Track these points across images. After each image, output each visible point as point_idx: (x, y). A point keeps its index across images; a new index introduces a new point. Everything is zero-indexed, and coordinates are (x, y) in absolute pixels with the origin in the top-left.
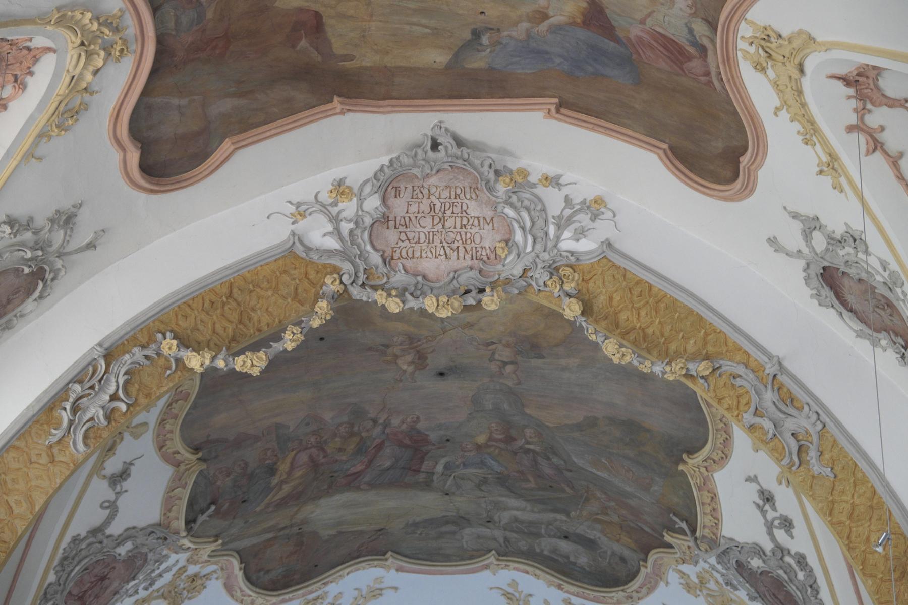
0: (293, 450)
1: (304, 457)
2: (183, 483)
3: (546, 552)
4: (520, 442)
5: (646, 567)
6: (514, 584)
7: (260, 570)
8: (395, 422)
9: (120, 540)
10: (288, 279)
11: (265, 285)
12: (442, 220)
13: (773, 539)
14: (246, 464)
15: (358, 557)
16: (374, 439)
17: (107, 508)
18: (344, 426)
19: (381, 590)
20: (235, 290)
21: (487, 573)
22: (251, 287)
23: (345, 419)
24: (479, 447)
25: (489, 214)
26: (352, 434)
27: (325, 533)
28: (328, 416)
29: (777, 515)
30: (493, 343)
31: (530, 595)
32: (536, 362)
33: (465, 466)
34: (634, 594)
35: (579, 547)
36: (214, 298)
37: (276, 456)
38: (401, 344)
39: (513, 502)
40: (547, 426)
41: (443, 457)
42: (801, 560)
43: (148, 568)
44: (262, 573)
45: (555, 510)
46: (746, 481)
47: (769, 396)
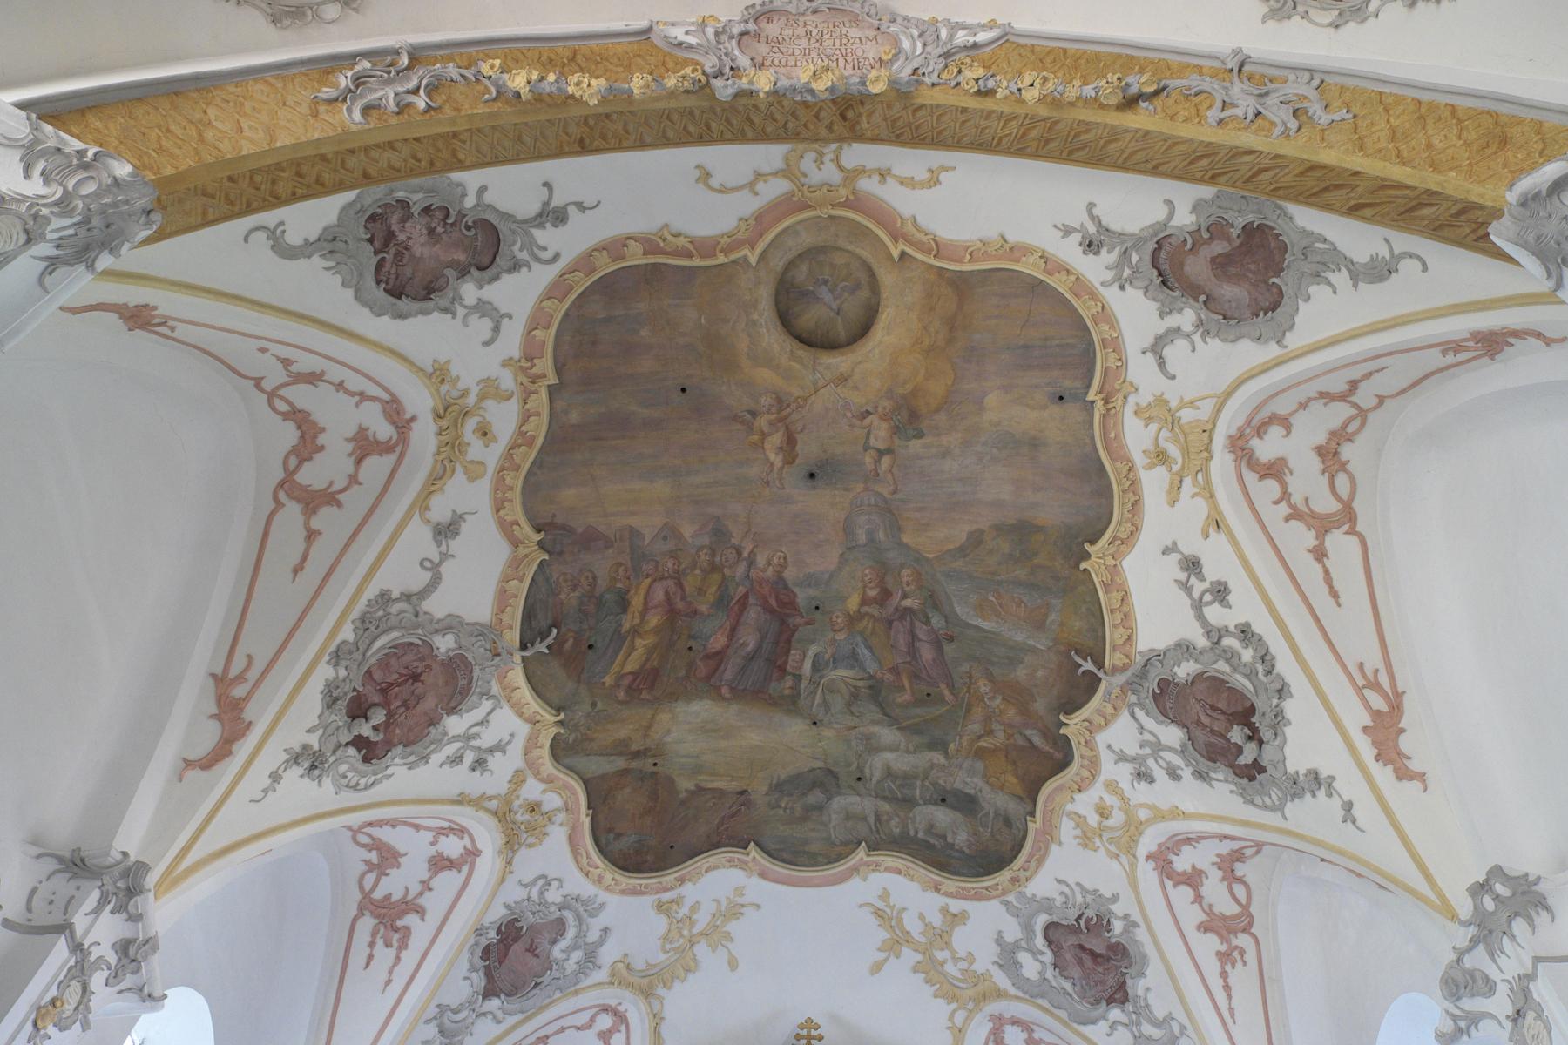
0: (648, 576)
1: (659, 595)
2: (521, 573)
3: (921, 835)
4: (895, 599)
5: (1035, 822)
6: (885, 895)
7: (610, 830)
8: (761, 560)
10: (643, 63)
11: (615, 60)
12: (820, 41)
14: (595, 578)
15: (717, 848)
16: (738, 584)
17: (427, 569)
18: (705, 551)
19: (743, 906)
20: (579, 57)
22: (598, 59)
23: (706, 540)
24: (853, 619)
25: (871, 33)
26: (714, 568)
28: (687, 531)
29: (1207, 585)
30: (868, 413)
31: (904, 909)
32: (915, 445)
34: (1022, 874)
36: (553, 56)
37: (629, 579)
39: (887, 735)
40: (927, 560)
41: (812, 642)
42: (1245, 633)
46: (1163, 553)
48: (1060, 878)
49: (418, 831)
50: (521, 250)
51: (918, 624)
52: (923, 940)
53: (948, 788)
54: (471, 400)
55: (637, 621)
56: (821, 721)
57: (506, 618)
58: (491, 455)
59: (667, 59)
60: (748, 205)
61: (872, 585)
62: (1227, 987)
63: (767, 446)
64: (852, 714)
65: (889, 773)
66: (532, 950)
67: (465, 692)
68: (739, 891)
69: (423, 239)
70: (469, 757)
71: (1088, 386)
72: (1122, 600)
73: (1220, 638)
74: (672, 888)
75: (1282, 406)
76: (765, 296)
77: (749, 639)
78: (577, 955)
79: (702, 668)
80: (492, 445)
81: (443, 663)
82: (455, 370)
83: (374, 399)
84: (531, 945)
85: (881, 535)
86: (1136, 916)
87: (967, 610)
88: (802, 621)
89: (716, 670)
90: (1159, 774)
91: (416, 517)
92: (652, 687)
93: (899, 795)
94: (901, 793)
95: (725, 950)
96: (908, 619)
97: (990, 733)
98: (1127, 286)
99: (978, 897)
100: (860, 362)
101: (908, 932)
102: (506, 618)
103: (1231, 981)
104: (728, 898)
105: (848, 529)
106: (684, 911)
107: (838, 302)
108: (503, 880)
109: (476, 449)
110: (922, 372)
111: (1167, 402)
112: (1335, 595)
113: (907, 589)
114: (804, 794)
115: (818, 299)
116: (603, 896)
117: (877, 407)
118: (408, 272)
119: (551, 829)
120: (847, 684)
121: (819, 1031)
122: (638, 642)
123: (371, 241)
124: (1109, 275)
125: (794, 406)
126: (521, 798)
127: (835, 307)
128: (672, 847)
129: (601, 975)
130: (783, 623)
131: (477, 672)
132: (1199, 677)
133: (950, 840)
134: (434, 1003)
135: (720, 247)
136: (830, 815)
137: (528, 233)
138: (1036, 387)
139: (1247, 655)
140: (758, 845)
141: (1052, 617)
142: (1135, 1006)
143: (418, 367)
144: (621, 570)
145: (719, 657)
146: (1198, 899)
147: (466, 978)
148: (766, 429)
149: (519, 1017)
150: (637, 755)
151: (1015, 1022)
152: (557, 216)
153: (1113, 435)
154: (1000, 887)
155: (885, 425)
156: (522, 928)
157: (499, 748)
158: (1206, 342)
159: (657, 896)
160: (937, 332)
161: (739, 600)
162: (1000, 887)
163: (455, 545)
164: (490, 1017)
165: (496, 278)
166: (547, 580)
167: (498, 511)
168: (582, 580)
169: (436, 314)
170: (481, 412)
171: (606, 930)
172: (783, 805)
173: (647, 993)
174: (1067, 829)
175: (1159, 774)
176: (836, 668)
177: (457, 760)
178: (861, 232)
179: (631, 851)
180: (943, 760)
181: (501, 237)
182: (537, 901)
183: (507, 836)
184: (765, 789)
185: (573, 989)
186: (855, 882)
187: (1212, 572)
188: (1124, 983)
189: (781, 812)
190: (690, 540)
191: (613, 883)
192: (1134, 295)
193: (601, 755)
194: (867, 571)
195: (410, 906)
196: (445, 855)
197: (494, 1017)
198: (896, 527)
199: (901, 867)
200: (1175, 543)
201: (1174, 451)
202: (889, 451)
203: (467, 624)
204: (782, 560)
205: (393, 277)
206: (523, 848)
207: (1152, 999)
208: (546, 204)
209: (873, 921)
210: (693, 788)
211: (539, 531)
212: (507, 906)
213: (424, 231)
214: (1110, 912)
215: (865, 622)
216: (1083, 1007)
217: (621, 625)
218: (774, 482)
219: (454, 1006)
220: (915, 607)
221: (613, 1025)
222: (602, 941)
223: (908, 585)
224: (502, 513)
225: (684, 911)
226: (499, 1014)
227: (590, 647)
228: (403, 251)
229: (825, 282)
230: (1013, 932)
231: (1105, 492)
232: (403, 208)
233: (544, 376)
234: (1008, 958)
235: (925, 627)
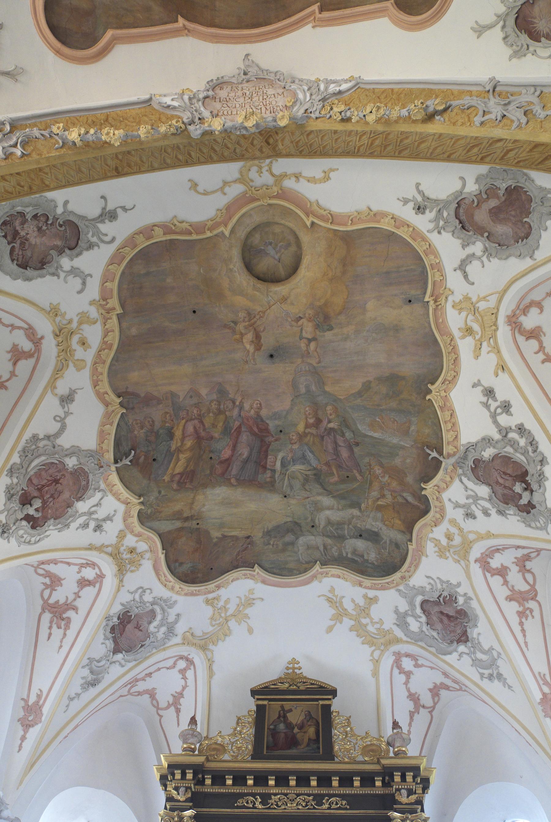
0: (183, 418)
1: (190, 429)
2: (111, 421)
3: (349, 556)
4: (325, 422)
6: (332, 590)
7: (176, 561)
8: (247, 406)
10: (147, 119)
11: (131, 119)
14: (153, 421)
15: (237, 568)
16: (235, 420)
18: (215, 402)
19: (254, 599)
20: (110, 119)
22: (121, 119)
23: (215, 396)
24: (302, 437)
26: (220, 412)
28: (204, 392)
29: (498, 404)
30: (301, 318)
31: (344, 597)
32: (329, 335)
34: (407, 574)
35: (369, 543)
36: (94, 119)
37: (172, 421)
38: (244, 321)
39: (326, 501)
40: (340, 400)
41: (280, 451)
44: (177, 564)
46: (473, 387)
48: (427, 575)
49: (70, 566)
50: (93, 236)
51: (338, 437)
52: (354, 613)
53: (363, 528)
54: (74, 325)
55: (179, 444)
56: (289, 495)
57: (104, 446)
58: (89, 356)
59: (162, 116)
60: (221, 201)
61: (311, 416)
62: (523, 631)
63: (244, 341)
64: (306, 490)
65: (329, 522)
66: (138, 627)
67: (86, 488)
68: (251, 591)
69: (35, 234)
70: (92, 524)
71: (425, 293)
72: (451, 415)
73: (507, 433)
74: (213, 592)
75: (536, 296)
76: (236, 253)
77: (244, 452)
78: (163, 629)
79: (219, 469)
81: (71, 473)
82: (63, 308)
83: (19, 328)
84: (137, 625)
85: (313, 388)
86: (471, 594)
87: (365, 427)
88: (273, 439)
89: (226, 470)
90: (479, 514)
91: (50, 391)
92: (191, 481)
93: (336, 534)
94: (337, 533)
95: (246, 624)
96: (332, 434)
97: (383, 496)
98: (442, 231)
99: (383, 588)
100: (294, 289)
101: (346, 610)
102: (104, 446)
103: (525, 627)
104: (245, 596)
105: (294, 385)
106: (221, 603)
107: (279, 254)
108: (118, 590)
109: (79, 353)
111: (470, 299)
113: (331, 417)
114: (283, 536)
115: (267, 254)
116: (175, 597)
117: (305, 314)
118: (29, 253)
119: (143, 562)
121: (299, 665)
122: (182, 456)
123: (5, 236)
124: (431, 226)
125: (258, 317)
126: (125, 546)
127: (277, 257)
128: (212, 569)
129: (177, 640)
130: (262, 441)
131: (91, 477)
132: (495, 457)
133: (366, 557)
134: (87, 657)
135: (207, 227)
136: (298, 547)
137: (95, 227)
138: (395, 295)
139: (522, 442)
140: (260, 565)
141: (413, 428)
142: (472, 643)
143: (41, 308)
144: (168, 416)
145: (228, 462)
146: (506, 583)
147: (103, 643)
148: (243, 331)
149: (134, 663)
150: (187, 519)
151: (407, 655)
152: (112, 216)
153: (441, 320)
154: (395, 582)
155: (310, 324)
156: (131, 615)
157: (109, 518)
158: (490, 261)
159: (205, 596)
160: (336, 268)
161: (236, 430)
162: (395, 582)
163: (73, 407)
164: (117, 664)
165: (78, 255)
166: (126, 424)
167: (95, 387)
168: (146, 423)
169: (48, 277)
170: (81, 332)
171: (178, 615)
172: (272, 543)
173: (204, 648)
174: (430, 548)
175: (479, 514)
176: (294, 465)
177: (85, 526)
178: (287, 212)
179: (189, 572)
180: (359, 514)
181: (80, 230)
182: (139, 601)
183: (119, 566)
184: (260, 534)
185: (162, 647)
186: (315, 583)
187: (501, 396)
188: (466, 631)
189: (271, 547)
190: (205, 397)
191: (180, 590)
192: (446, 236)
193: (168, 520)
194: (307, 409)
195: (69, 606)
196: (86, 578)
198: (321, 383)
199: (340, 574)
200: (479, 381)
201: (476, 327)
202: (314, 339)
203: (83, 451)
204: (259, 405)
205: (21, 257)
206: (129, 572)
207: (481, 639)
208: (104, 209)
209: (327, 604)
210: (220, 536)
211: (119, 397)
212: (122, 604)
213: (36, 229)
214: (456, 592)
215: (308, 438)
216: (444, 646)
217: (170, 447)
218: (250, 361)
219: (97, 659)
220: (336, 427)
221: (187, 666)
222: (176, 621)
223: (331, 415)
224: (97, 388)
225: (221, 603)
226: (123, 662)
227: (154, 460)
228: (24, 241)
229: (271, 244)
230: (403, 606)
231: (438, 354)
232: (21, 216)
233: (114, 309)
235: (342, 438)
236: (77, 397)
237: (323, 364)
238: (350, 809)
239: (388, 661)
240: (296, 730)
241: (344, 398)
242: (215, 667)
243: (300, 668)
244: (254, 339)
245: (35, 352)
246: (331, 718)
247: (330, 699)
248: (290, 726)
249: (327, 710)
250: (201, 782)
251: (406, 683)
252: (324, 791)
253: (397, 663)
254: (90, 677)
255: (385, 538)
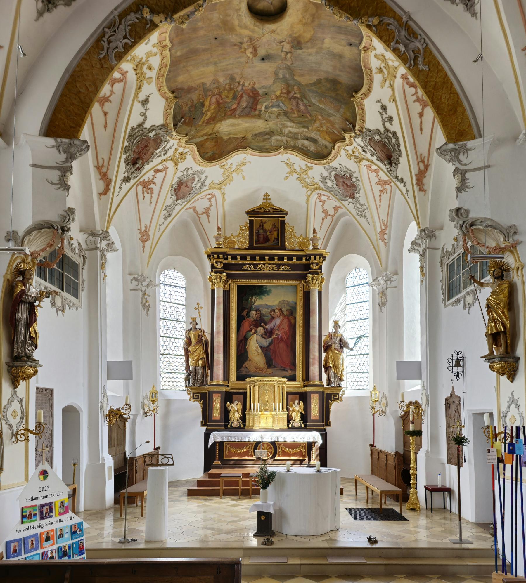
4: (292, 94)
6: (289, 159)
7: (204, 152)
9: (150, 130)
13: (385, 127)
15: (237, 149)
17: (143, 116)
21: (280, 155)
23: (228, 81)
24: (277, 97)
27: (226, 138)
30: (283, 41)
31: (294, 164)
32: (299, 52)
33: (272, 107)
35: (311, 143)
38: (247, 42)
39: (289, 124)
40: (303, 85)
41: (265, 102)
43: (163, 145)
45: (304, 127)
47: (403, 33)
51: (299, 101)
52: (300, 172)
54: (144, 60)
58: (153, 74)
64: (278, 118)
65: (290, 132)
66: (187, 186)
80: (153, 71)
85: (287, 76)
105: (276, 73)
109: (149, 74)
110: (302, 30)
112: (421, 130)
114: (264, 136)
116: (204, 169)
120: (276, 112)
147: (171, 198)
148: (246, 48)
150: (210, 134)
160: (308, 19)
163: (148, 106)
180: (307, 130)
190: (222, 82)
195: (151, 182)
197: (180, 204)
202: (290, 52)
209: (285, 166)
212: (178, 178)
216: (342, 197)
220: (299, 97)
224: (161, 91)
226: (181, 203)
230: (325, 174)
234: (324, 180)
236: (150, 99)
237: (294, 65)
238: (291, 271)
239: (315, 196)
240: (268, 233)
241: (305, 85)
242: (226, 196)
243: (270, 199)
244: (253, 51)
245: (123, 79)
246: (284, 227)
247: (284, 217)
248: (265, 231)
249: (283, 223)
250: (227, 259)
251: (322, 206)
252: (280, 262)
253: (319, 197)
254: (167, 214)
255: (320, 143)
